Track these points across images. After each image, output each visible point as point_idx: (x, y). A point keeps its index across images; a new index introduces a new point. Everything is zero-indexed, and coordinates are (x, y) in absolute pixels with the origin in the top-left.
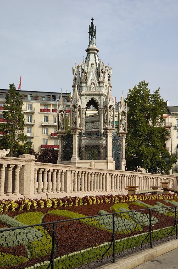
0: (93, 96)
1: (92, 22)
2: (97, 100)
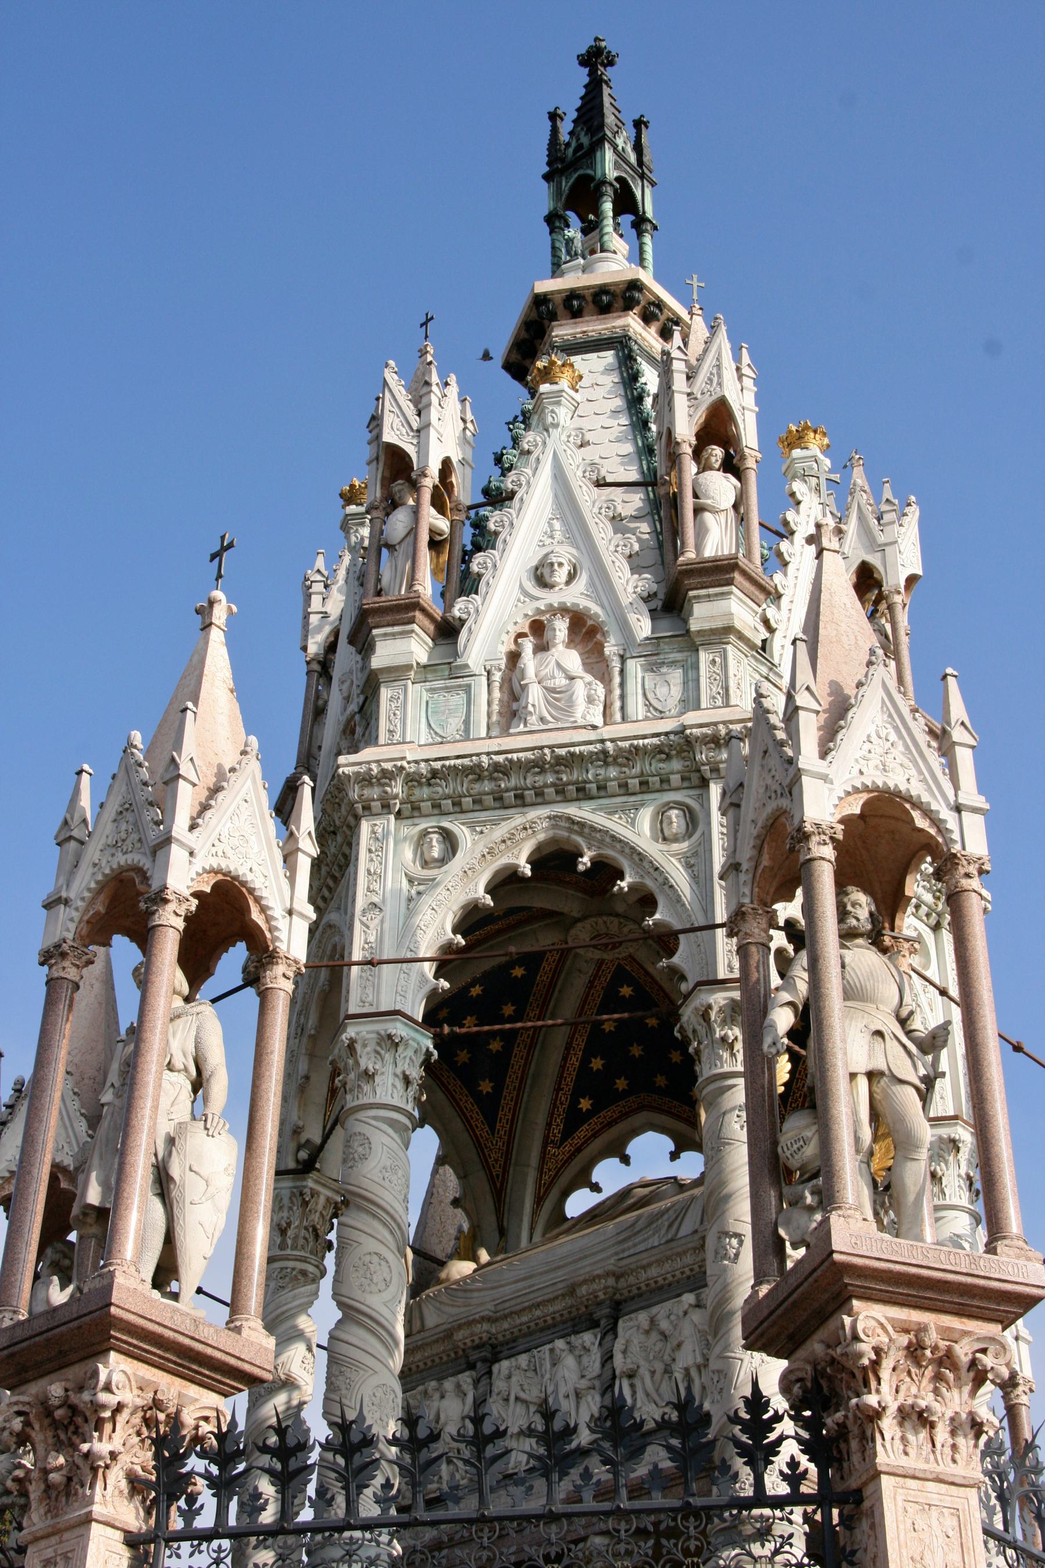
0: (562, 793)
2: (638, 857)
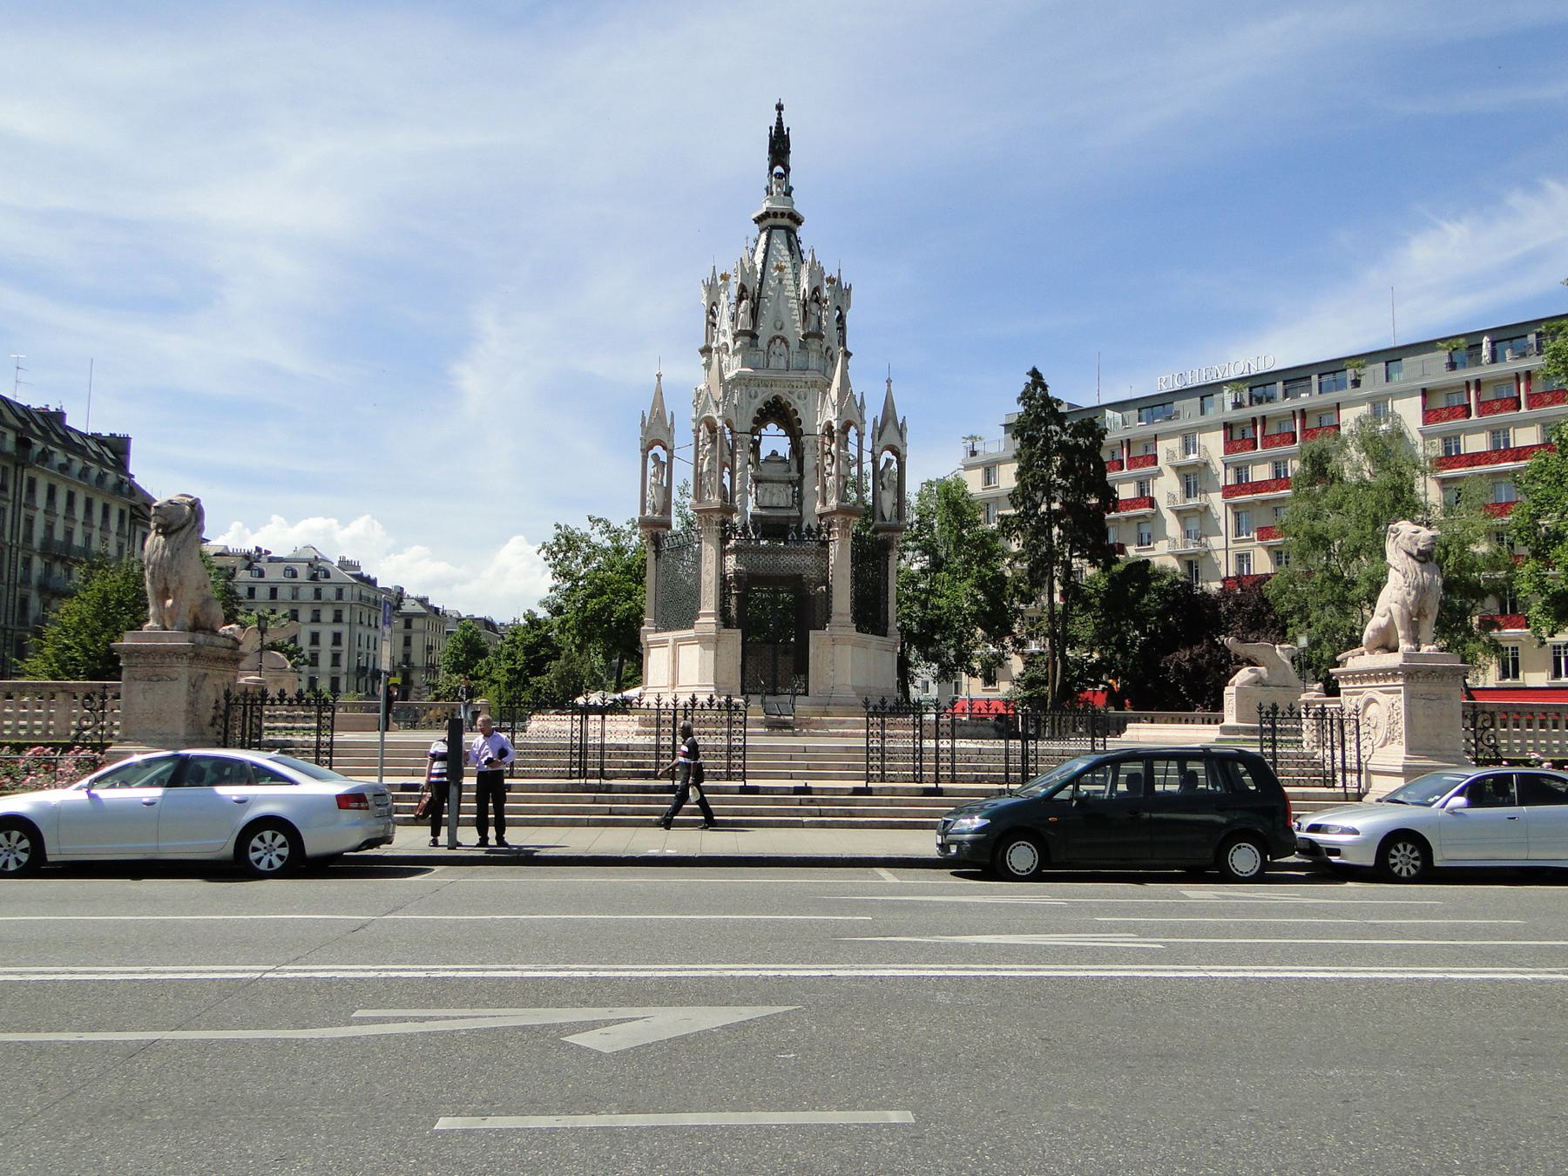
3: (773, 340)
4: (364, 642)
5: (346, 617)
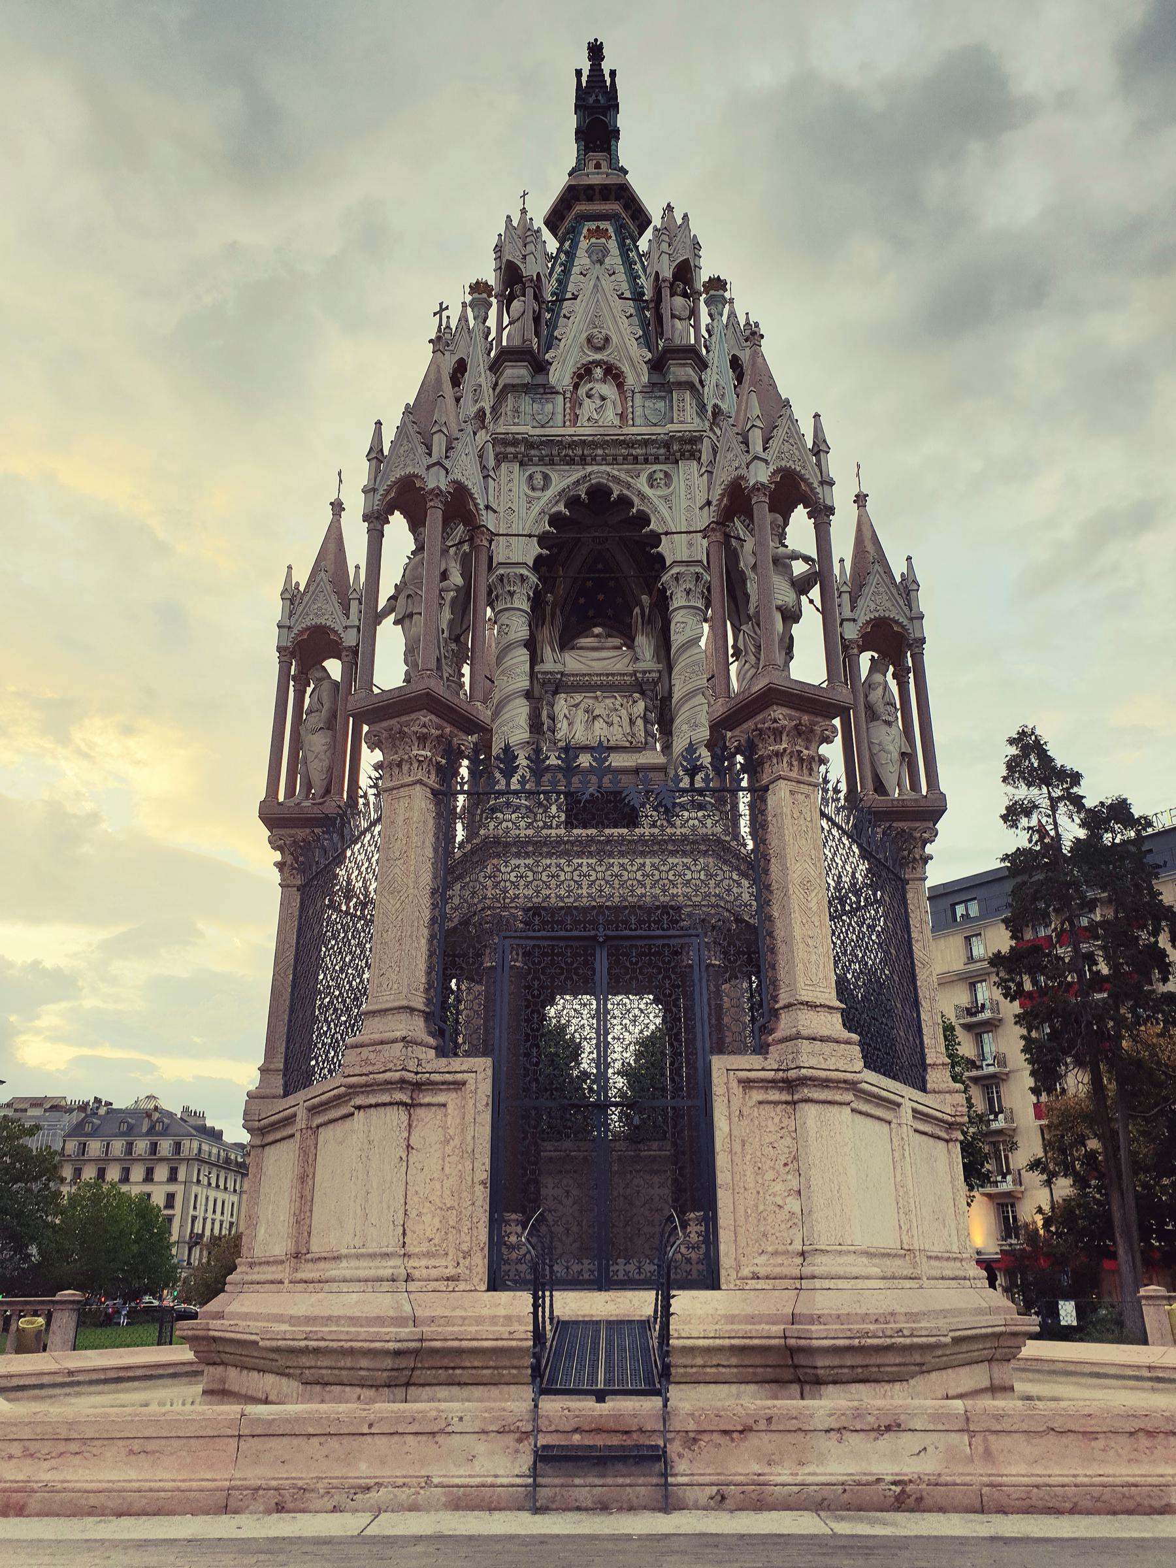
1: (596, 70)
2: (641, 495)
3: (584, 374)
4: (201, 1200)
5: (181, 1176)
